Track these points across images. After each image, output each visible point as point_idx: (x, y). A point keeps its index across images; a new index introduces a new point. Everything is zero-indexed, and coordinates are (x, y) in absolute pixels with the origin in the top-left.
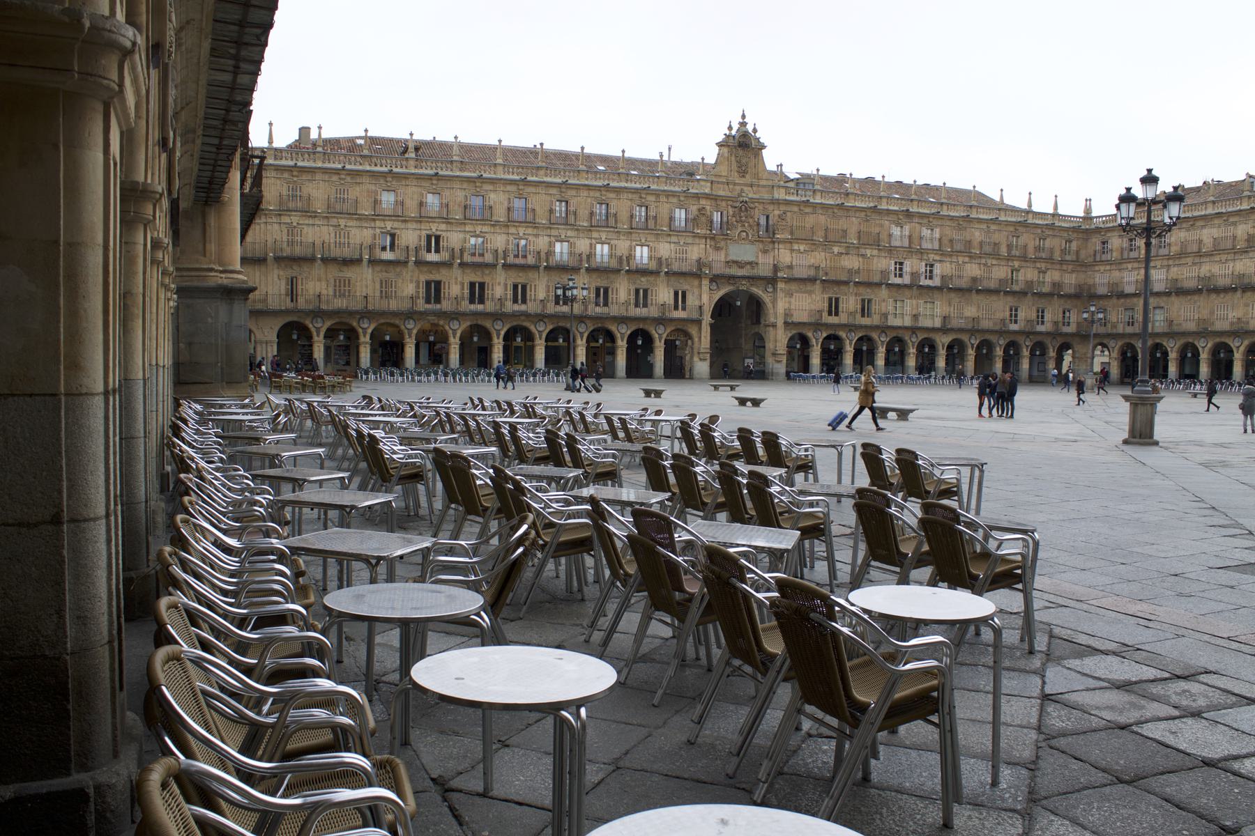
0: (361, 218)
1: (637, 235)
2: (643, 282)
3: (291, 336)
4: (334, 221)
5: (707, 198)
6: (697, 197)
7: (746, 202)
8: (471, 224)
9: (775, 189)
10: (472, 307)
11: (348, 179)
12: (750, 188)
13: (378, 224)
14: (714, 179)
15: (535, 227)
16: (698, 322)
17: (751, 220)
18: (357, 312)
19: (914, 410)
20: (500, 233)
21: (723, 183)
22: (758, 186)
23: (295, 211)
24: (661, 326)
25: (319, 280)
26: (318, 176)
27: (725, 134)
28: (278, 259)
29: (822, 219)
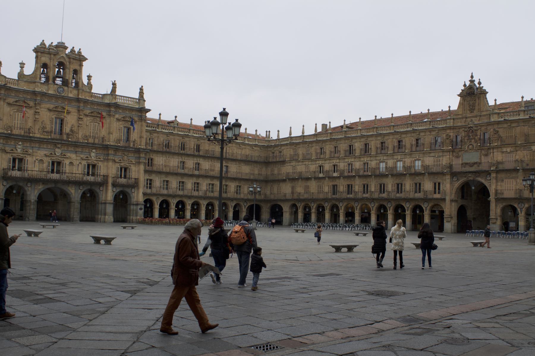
0: (313, 161)
1: (414, 155)
2: (418, 179)
3: (209, 208)
4: (304, 163)
5: (450, 129)
6: (444, 129)
7: (471, 127)
8: (347, 158)
9: (491, 116)
10: (348, 196)
11: (310, 145)
12: (476, 118)
13: (318, 162)
14: (455, 117)
15: (371, 157)
16: (444, 200)
17: (476, 138)
18: (310, 200)
19: (357, 246)
20: (357, 161)
21: (460, 118)
22: (480, 116)
23: (293, 160)
24: (425, 203)
25: (300, 187)
26: (301, 146)
27: (462, 90)
28: (289, 179)
29: (526, 129)
